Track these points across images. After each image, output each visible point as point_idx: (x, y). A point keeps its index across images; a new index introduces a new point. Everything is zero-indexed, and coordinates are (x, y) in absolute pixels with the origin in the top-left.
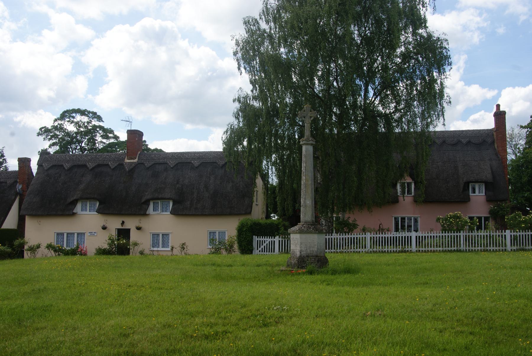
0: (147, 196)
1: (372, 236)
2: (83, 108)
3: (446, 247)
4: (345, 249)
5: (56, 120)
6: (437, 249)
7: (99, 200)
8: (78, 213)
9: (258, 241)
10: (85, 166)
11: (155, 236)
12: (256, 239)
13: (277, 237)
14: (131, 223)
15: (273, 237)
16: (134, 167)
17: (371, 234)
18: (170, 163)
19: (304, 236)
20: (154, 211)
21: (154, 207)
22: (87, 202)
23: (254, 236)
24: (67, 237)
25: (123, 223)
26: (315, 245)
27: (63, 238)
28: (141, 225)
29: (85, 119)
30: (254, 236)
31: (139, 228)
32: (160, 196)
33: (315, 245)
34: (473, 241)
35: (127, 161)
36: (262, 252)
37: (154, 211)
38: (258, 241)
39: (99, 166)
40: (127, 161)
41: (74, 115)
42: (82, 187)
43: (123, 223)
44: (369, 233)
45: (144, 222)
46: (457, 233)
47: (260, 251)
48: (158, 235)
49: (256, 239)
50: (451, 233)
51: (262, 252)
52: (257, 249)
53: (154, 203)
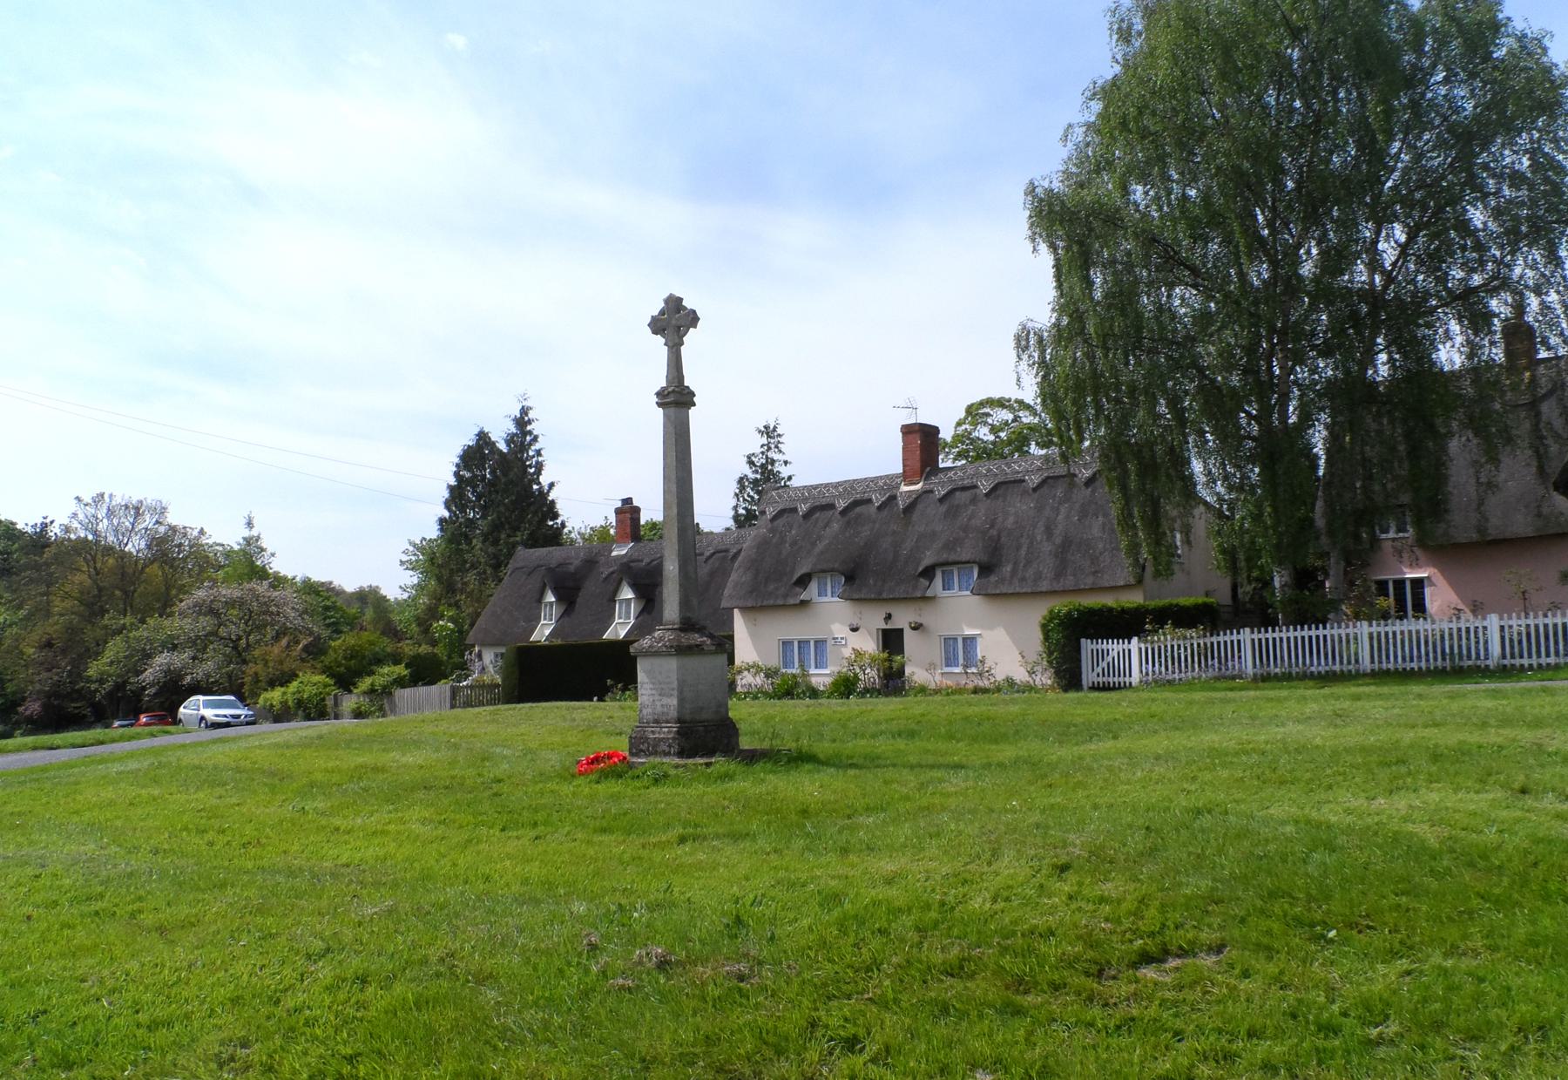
0: (928, 559)
1: (1375, 629)
2: (996, 395)
3: (1521, 657)
4: (1173, 672)
5: (959, 424)
6: (1513, 661)
7: (843, 574)
8: (939, 595)
9: (1092, 650)
10: (831, 506)
11: (949, 641)
12: (1087, 646)
13: (1135, 640)
14: (903, 618)
15: (1126, 641)
16: (916, 499)
17: (1371, 625)
18: (983, 485)
19: (694, 663)
20: (944, 589)
21: (943, 581)
22: (826, 578)
23: (1083, 640)
24: (799, 647)
25: (889, 617)
26: (673, 689)
27: (793, 651)
28: (919, 620)
29: (1007, 415)
30: (1083, 640)
31: (917, 627)
32: (952, 557)
33: (673, 689)
34: (1384, 653)
35: (904, 488)
36: (1104, 675)
37: (944, 589)
38: (1092, 650)
39: (856, 503)
40: (904, 488)
41: (987, 410)
42: (820, 546)
43: (889, 617)
44: (1365, 624)
45: (927, 616)
46: (1212, 635)
47: (1098, 675)
48: (955, 639)
49: (1087, 646)
50: (1339, 627)
51: (1104, 675)
52: (1093, 670)
53: (943, 572)
